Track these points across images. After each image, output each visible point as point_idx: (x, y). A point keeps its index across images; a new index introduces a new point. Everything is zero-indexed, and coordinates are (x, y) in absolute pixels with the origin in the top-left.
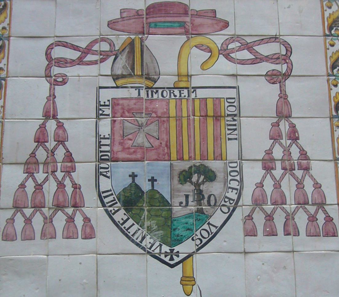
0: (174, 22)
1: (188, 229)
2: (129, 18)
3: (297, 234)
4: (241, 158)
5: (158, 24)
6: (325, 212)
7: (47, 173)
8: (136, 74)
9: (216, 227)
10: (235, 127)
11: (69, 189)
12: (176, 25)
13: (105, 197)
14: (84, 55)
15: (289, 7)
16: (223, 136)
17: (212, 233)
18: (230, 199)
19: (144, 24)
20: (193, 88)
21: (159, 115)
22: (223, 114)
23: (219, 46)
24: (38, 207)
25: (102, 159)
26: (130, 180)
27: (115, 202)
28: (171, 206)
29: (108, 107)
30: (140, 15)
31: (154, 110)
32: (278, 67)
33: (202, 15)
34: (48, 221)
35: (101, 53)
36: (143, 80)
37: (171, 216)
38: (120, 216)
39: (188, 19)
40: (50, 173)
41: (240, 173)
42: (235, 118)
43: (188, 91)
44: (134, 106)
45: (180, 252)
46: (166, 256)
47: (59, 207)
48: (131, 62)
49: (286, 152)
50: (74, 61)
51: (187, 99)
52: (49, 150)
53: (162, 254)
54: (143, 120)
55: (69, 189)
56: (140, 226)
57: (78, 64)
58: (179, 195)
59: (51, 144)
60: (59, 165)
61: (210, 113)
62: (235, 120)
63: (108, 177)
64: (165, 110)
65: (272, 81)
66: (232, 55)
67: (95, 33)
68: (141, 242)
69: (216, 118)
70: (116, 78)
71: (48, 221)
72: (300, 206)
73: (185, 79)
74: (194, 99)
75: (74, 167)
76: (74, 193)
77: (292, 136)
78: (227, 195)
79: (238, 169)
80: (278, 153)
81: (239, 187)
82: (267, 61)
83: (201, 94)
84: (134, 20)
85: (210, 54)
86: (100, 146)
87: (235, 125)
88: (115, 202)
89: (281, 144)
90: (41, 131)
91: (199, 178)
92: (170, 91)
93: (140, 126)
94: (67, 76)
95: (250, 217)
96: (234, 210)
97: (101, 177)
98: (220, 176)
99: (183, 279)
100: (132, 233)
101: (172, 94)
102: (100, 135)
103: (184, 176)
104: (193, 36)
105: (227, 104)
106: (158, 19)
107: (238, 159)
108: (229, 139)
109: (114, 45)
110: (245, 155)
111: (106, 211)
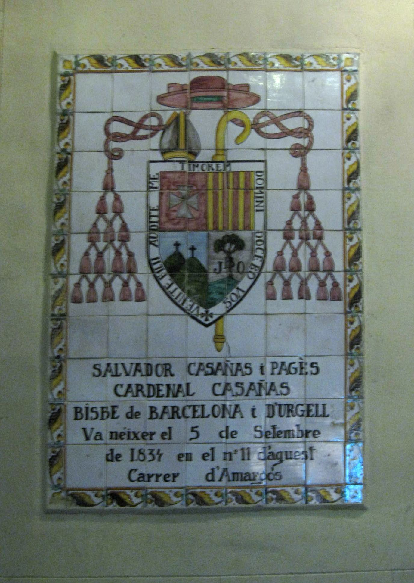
1: (221, 293)
3: (308, 297)
4: (266, 228)
6: (333, 278)
9: (243, 291)
10: (261, 199)
11: (125, 257)
13: (155, 264)
14: (136, 129)
15: (313, 81)
18: (256, 266)
21: (199, 187)
23: (252, 120)
24: (100, 272)
32: (300, 141)
33: (238, 89)
34: (108, 285)
35: (152, 127)
36: (185, 154)
38: (166, 281)
39: (225, 94)
41: (265, 242)
51: (223, 172)
55: (125, 257)
59: (110, 215)
60: (116, 235)
61: (242, 186)
62: (262, 193)
65: (295, 155)
66: (263, 129)
68: (182, 304)
70: (164, 152)
73: (221, 153)
79: (262, 239)
80: (297, 224)
83: (235, 167)
84: (178, 95)
89: (300, 216)
93: (183, 198)
95: (270, 283)
97: (151, 246)
98: (248, 244)
100: (175, 296)
101: (210, 168)
104: (230, 110)
105: (256, 177)
108: (257, 211)
110: (270, 226)
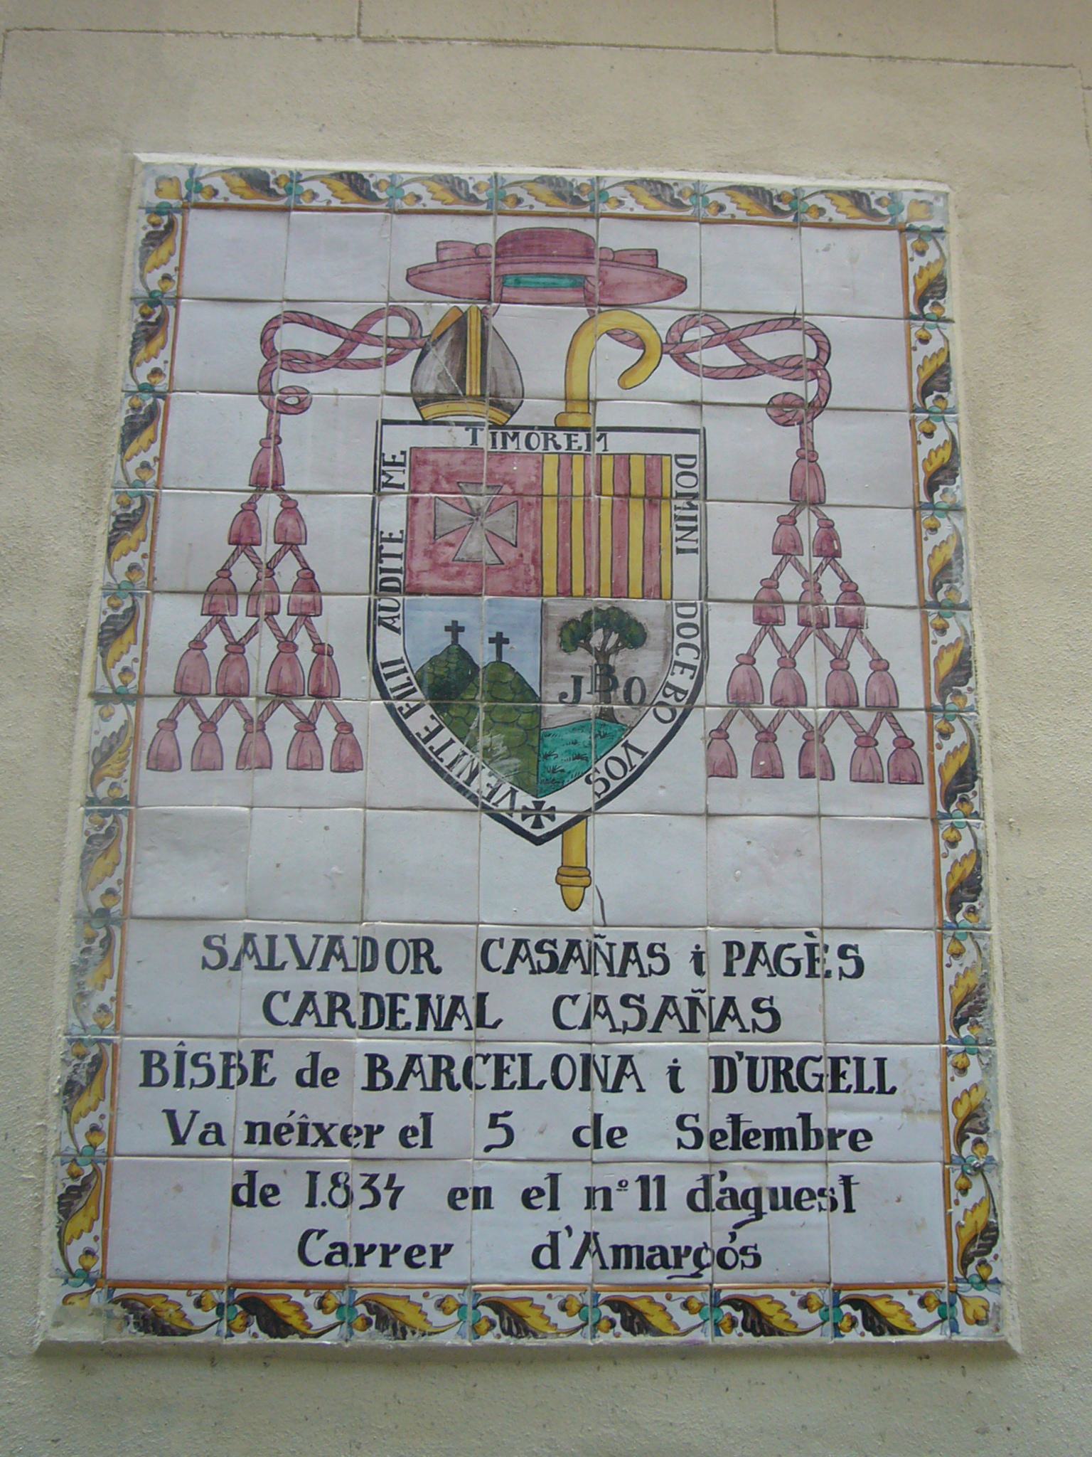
0: (560, 276)
1: (578, 757)
2: (458, 263)
3: (829, 775)
4: (704, 595)
5: (524, 279)
6: (896, 726)
7: (257, 616)
8: (468, 393)
9: (643, 754)
10: (693, 524)
11: (306, 655)
12: (565, 282)
13: (388, 676)
14: (349, 344)
15: (826, 250)
16: (665, 544)
17: (632, 768)
18: (677, 690)
19: (490, 279)
20: (599, 429)
21: (520, 489)
22: (666, 493)
23: (663, 334)
24: (233, 693)
25: (383, 589)
26: (447, 640)
27: (411, 687)
28: (540, 701)
29: (402, 468)
30: (482, 257)
31: (507, 478)
32: (797, 388)
33: (624, 260)
34: (255, 727)
35: (389, 342)
36: (484, 408)
37: (539, 726)
38: (422, 721)
39: (592, 270)
40: (263, 616)
41: (703, 629)
42: (694, 502)
43: (588, 436)
44: (462, 468)
45: (557, 809)
46: (524, 818)
47: (281, 696)
48: (458, 365)
49: (809, 586)
50: (326, 358)
51: (585, 455)
52: (261, 563)
53: (517, 811)
54: (479, 501)
55: (306, 655)
56: (468, 746)
57: (336, 366)
58: (559, 678)
59: (267, 549)
60: (284, 598)
61: (638, 488)
62: (693, 507)
63: (397, 630)
64: (533, 479)
65: (783, 419)
66: (693, 356)
67: (376, 295)
68: (468, 782)
69: (650, 501)
70: (421, 400)
71: (255, 727)
72: (837, 710)
73: (581, 408)
74: (601, 454)
75: (318, 605)
76: (317, 665)
77: (825, 547)
78: (671, 679)
79: (697, 620)
80: (791, 586)
81: (697, 663)
82: (771, 372)
83: (618, 443)
84: (467, 268)
85: (642, 351)
86: (380, 556)
87: (694, 519)
88: (411, 687)
89: (798, 567)
90: (244, 519)
91: (606, 638)
92: (546, 435)
93: (475, 514)
94: (308, 392)
95: (721, 733)
96: (685, 716)
97: (381, 629)
98: (656, 634)
99: (563, 871)
100: (447, 762)
101: (550, 443)
102: (382, 533)
103: (573, 633)
104: (603, 309)
105: (677, 470)
106: (524, 268)
107: (697, 597)
108: (679, 551)
109: (420, 324)
110: (716, 590)
111: (390, 708)
